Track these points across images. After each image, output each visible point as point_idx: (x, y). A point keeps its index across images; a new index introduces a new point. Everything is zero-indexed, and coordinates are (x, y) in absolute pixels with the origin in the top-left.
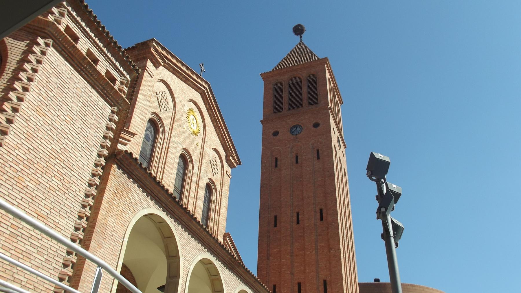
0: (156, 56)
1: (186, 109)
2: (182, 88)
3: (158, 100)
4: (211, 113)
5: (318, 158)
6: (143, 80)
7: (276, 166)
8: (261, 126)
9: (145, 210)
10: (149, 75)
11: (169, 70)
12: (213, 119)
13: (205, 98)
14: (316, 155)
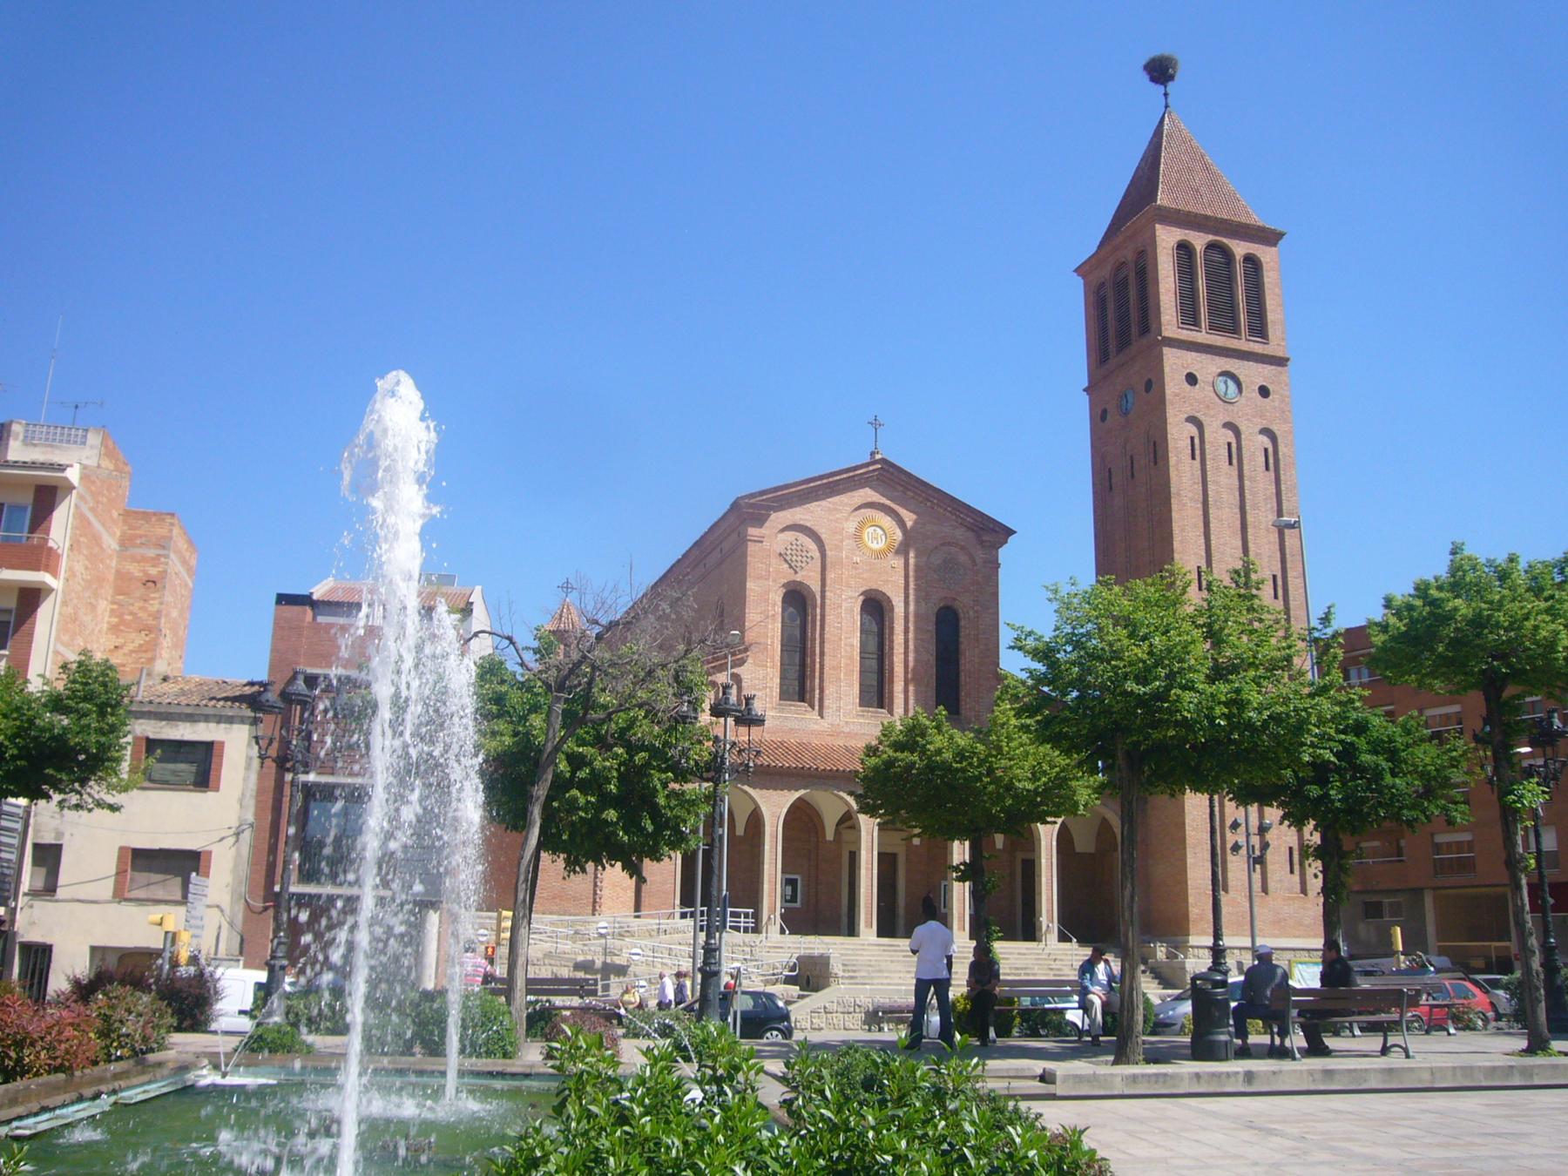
1: (851, 526)
3: (786, 560)
5: (1156, 463)
6: (749, 558)
7: (1111, 488)
8: (1085, 398)
14: (1152, 456)
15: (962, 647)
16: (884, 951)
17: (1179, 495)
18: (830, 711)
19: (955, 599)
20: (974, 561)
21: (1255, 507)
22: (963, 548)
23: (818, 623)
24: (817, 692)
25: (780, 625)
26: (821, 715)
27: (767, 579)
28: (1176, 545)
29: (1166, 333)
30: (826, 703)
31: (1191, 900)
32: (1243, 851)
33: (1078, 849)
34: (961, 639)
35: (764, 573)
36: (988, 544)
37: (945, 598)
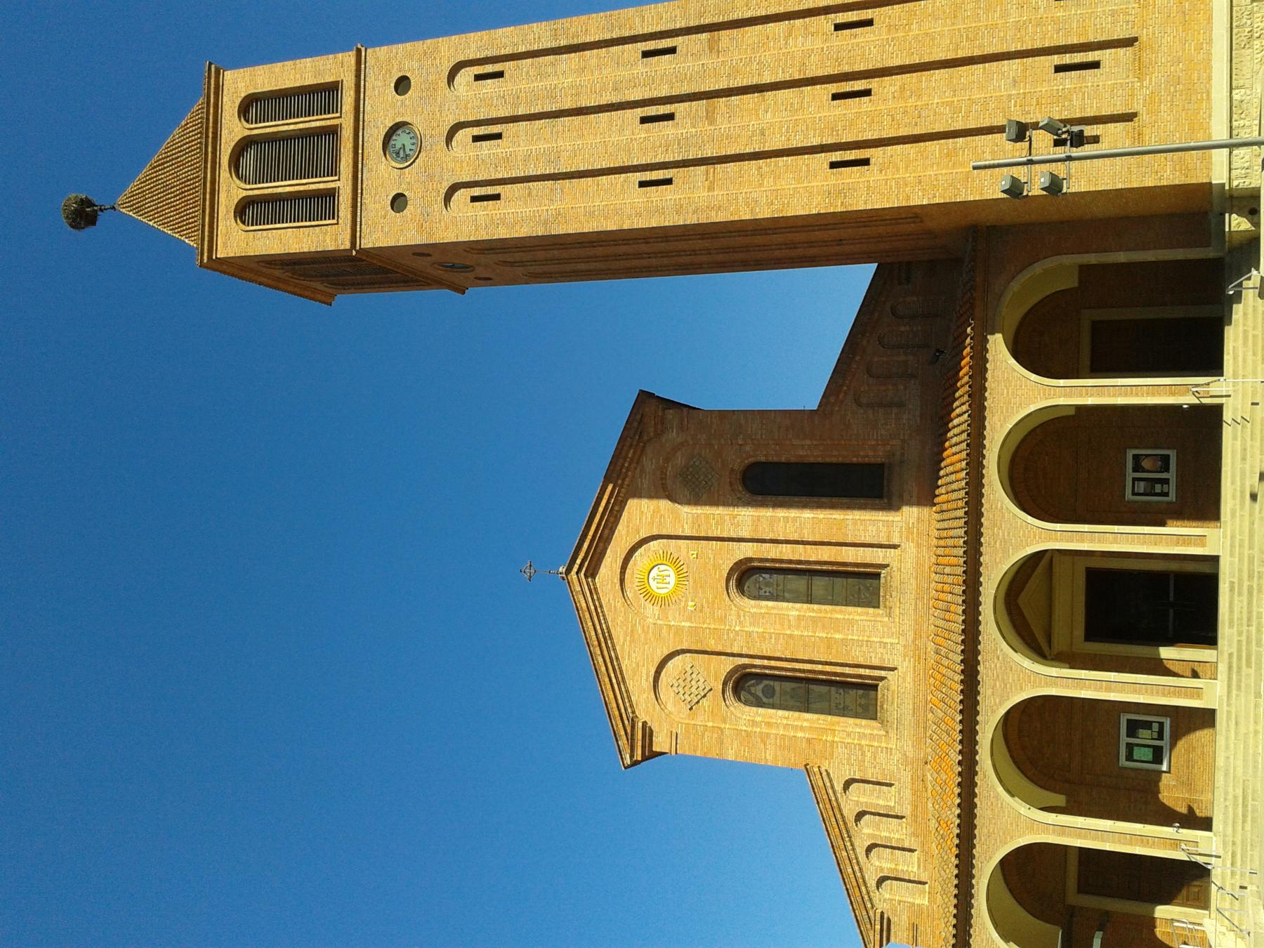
0: (640, 743)
1: (651, 611)
2: (628, 638)
3: (698, 702)
4: (607, 531)
9: (993, 937)
10: (678, 741)
11: (627, 691)
12: (612, 519)
13: (594, 563)
15: (793, 460)
16: (1239, 687)
17: (546, 223)
18: (886, 656)
19: (732, 470)
20: (682, 444)
21: (551, 95)
22: (667, 460)
23: (773, 663)
24: (862, 671)
25: (780, 713)
26: (893, 669)
27: (722, 730)
28: (611, 226)
29: (347, 245)
30: (876, 662)
31: (1149, 182)
32: (1060, 170)
33: (1076, 285)
34: (783, 460)
35: (715, 735)
36: (659, 427)
37: (731, 483)
